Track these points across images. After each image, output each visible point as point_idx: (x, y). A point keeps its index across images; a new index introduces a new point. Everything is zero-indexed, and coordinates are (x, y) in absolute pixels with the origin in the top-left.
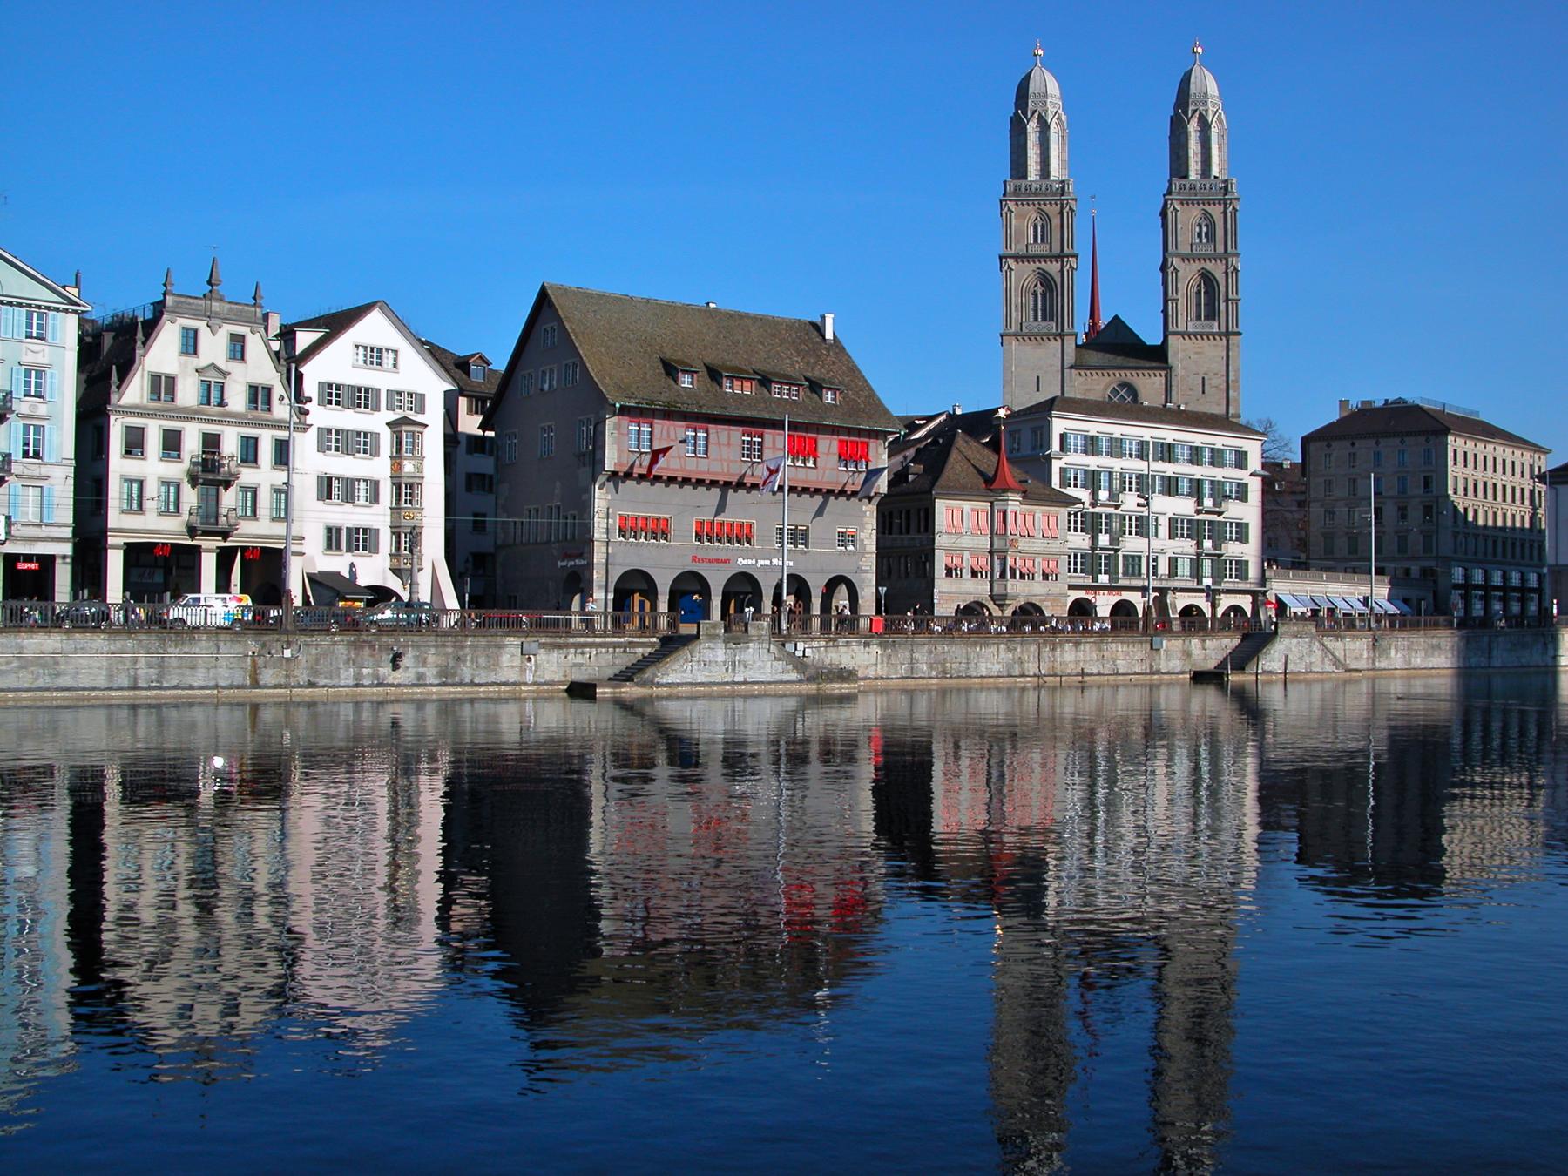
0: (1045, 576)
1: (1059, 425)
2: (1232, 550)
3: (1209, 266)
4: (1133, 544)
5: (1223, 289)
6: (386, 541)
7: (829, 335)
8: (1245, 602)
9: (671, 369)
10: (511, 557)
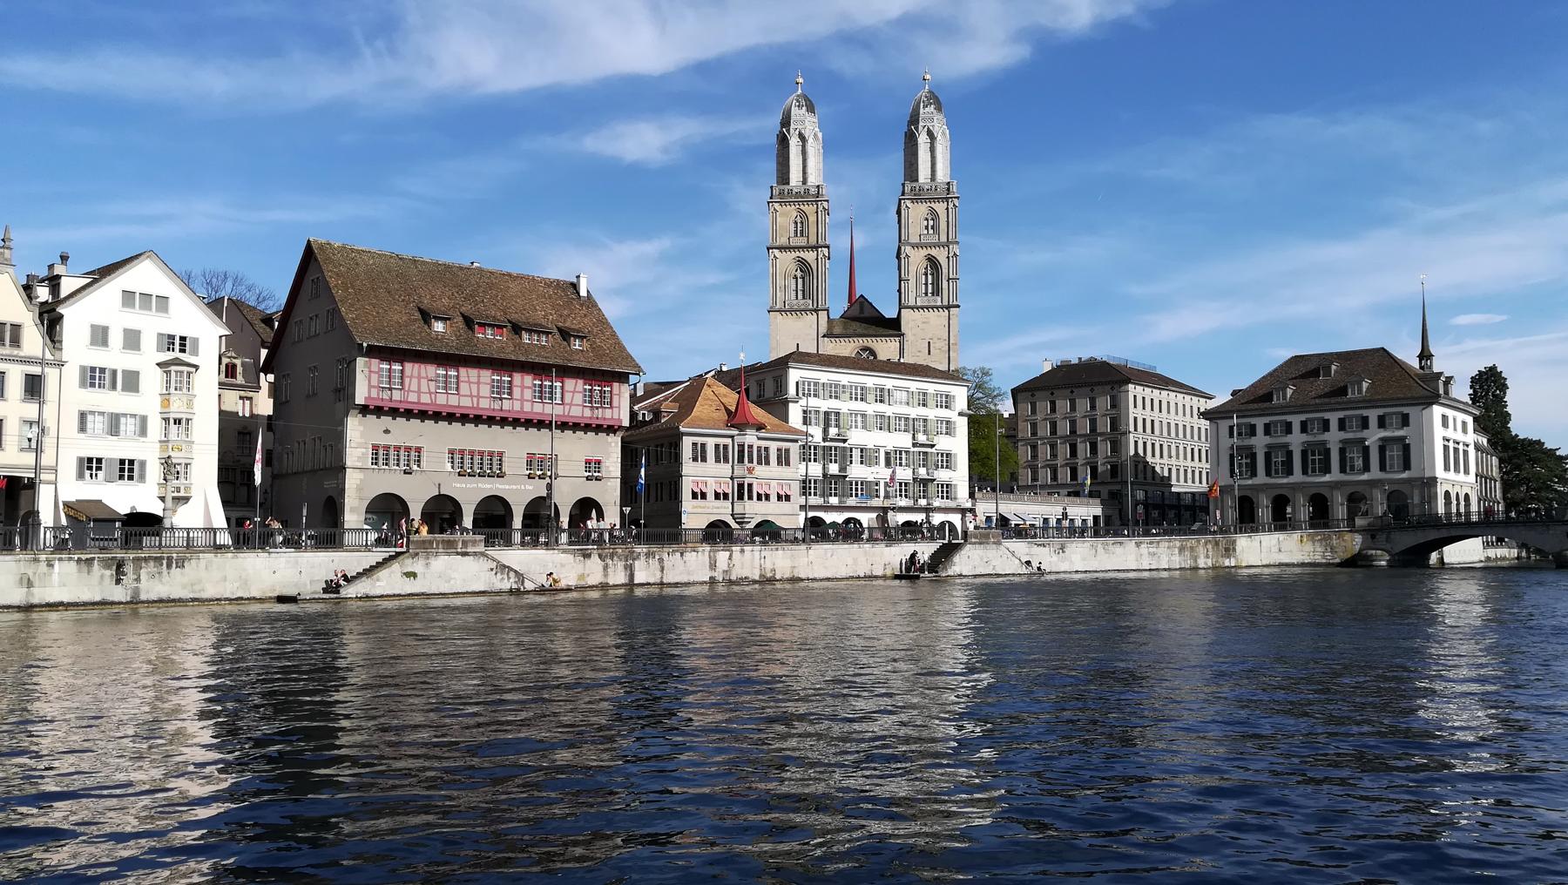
0: (779, 498)
1: (795, 375)
2: (942, 475)
3: (934, 252)
4: (857, 471)
5: (945, 271)
6: (154, 472)
7: (583, 293)
8: (956, 519)
9: (426, 317)
10: (276, 483)
